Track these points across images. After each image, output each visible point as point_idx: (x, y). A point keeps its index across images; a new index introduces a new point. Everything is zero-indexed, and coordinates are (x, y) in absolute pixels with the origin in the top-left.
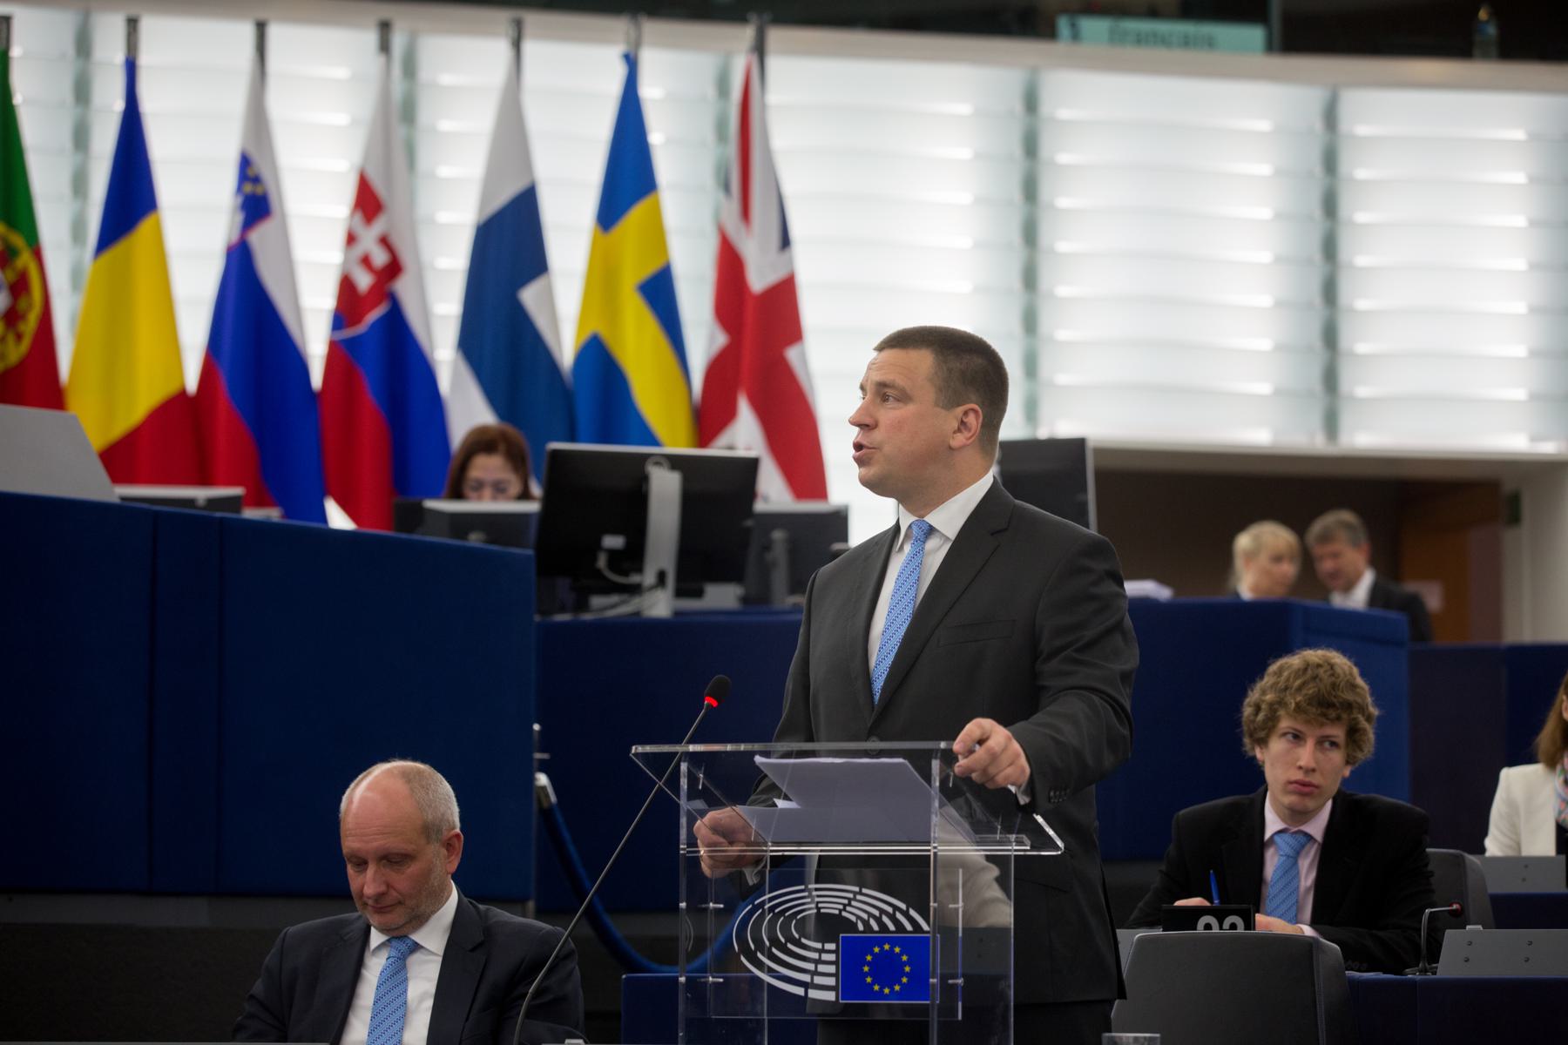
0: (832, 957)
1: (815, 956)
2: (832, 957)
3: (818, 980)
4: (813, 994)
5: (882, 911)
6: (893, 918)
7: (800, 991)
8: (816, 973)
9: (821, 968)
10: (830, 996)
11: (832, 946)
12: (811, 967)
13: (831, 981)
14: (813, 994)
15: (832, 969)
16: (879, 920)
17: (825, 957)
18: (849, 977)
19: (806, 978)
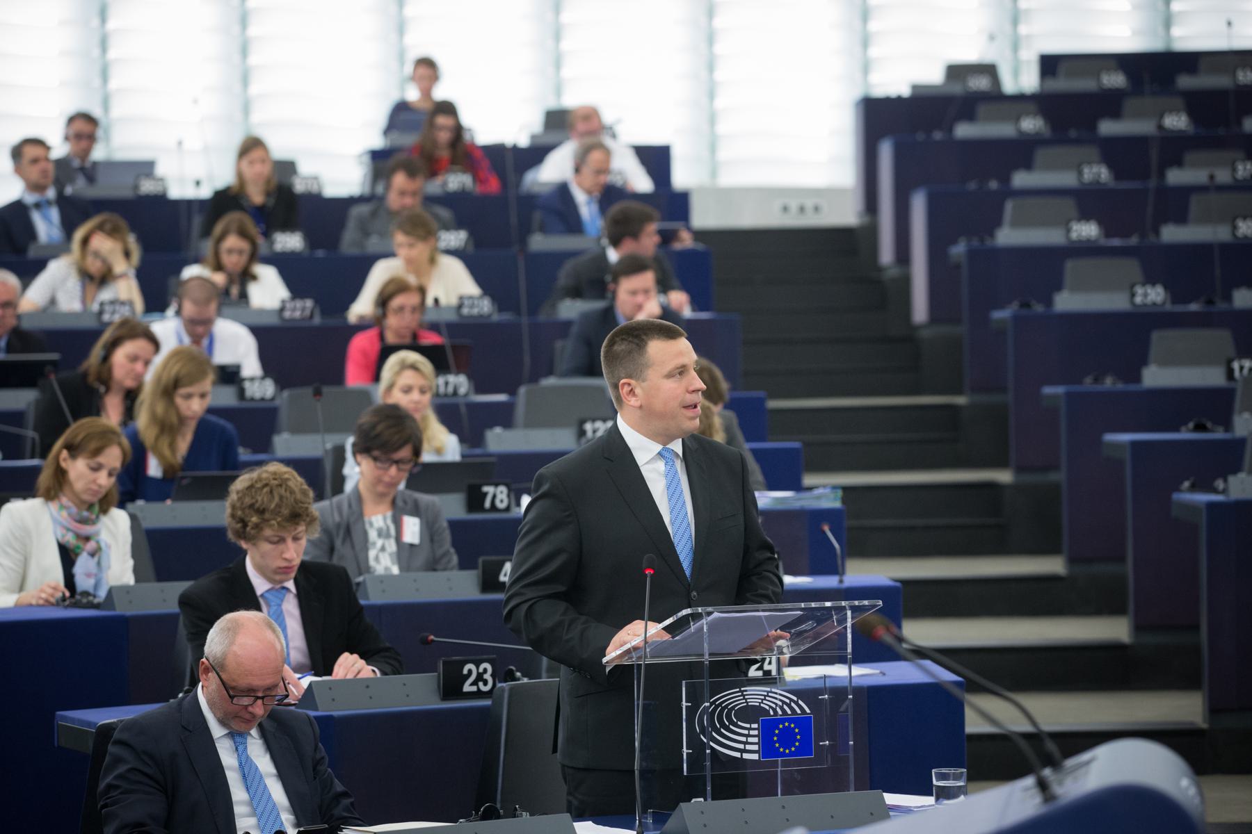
0: (756, 732)
1: (746, 732)
2: (756, 732)
3: (748, 747)
4: (746, 756)
5: (784, 702)
6: (789, 706)
7: (737, 755)
8: (745, 743)
9: (750, 740)
10: (755, 757)
11: (755, 726)
12: (744, 739)
13: (756, 748)
14: (746, 756)
15: (756, 740)
16: (782, 708)
17: (752, 732)
18: (767, 747)
19: (741, 746)
